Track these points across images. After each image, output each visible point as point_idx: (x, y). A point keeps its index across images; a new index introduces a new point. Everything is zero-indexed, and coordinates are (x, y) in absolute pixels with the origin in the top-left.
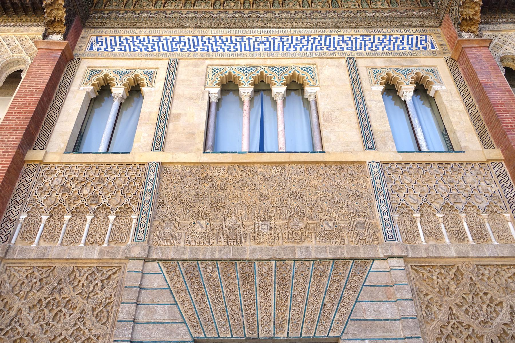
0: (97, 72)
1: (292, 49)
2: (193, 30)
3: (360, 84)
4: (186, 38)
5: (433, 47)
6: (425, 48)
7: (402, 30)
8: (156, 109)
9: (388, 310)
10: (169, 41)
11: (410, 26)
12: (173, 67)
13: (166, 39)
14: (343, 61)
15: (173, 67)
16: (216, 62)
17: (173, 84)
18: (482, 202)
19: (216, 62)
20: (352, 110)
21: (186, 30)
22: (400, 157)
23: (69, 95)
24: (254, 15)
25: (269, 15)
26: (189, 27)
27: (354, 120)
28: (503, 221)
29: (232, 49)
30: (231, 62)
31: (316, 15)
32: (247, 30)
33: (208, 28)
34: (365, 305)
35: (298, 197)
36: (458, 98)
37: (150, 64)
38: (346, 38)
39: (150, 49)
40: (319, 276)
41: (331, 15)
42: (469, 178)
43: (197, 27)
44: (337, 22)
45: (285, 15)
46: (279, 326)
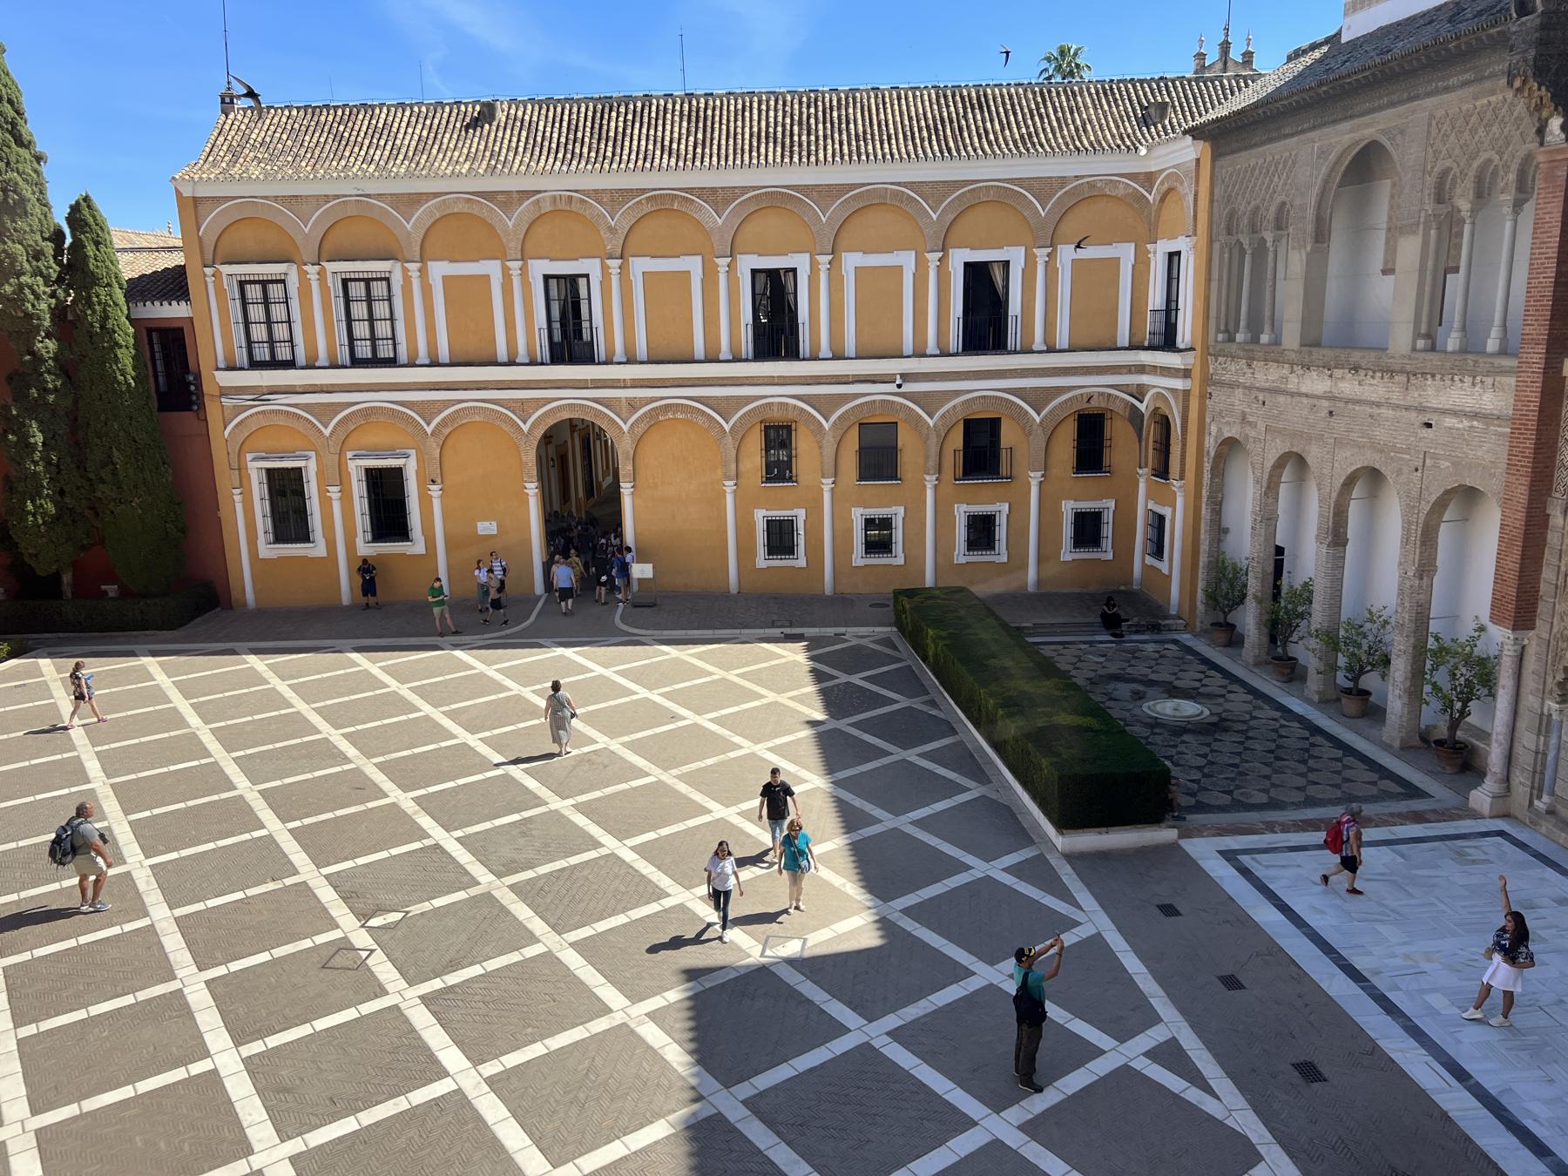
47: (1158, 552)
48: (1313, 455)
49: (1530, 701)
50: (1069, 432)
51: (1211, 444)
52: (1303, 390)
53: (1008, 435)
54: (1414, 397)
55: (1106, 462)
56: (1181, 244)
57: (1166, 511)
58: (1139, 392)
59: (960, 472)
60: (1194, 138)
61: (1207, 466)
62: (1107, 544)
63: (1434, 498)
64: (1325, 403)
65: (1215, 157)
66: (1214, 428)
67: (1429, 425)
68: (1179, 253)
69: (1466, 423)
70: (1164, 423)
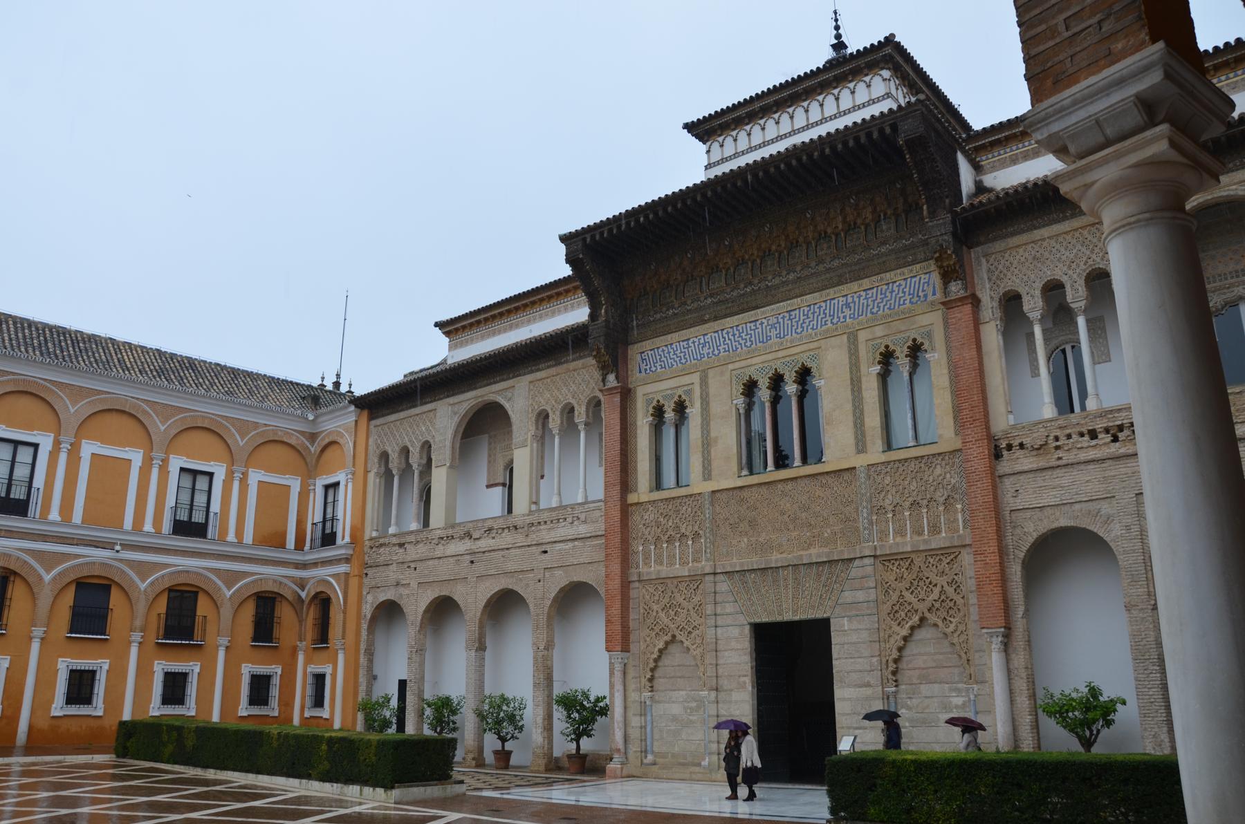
1: (799, 330)
2: (711, 324)
3: (859, 370)
5: (934, 294)
6: (925, 296)
7: (905, 270)
9: (860, 595)
11: (914, 262)
12: (704, 382)
14: (845, 337)
15: (704, 382)
16: (737, 365)
17: (708, 403)
18: (940, 496)
19: (737, 365)
20: (849, 407)
22: (883, 458)
23: (639, 432)
24: (762, 285)
25: (777, 281)
27: (851, 418)
28: (956, 511)
30: (749, 362)
31: (821, 268)
33: (726, 316)
34: (846, 594)
36: (946, 371)
37: (686, 380)
38: (850, 300)
40: (819, 576)
41: (836, 263)
42: (938, 471)
43: (716, 318)
44: (840, 276)
45: (791, 276)
46: (795, 612)
47: (319, 702)
48: (458, 593)
49: (633, 696)
50: (249, 611)
51: (368, 610)
52: (448, 552)
53: (203, 607)
54: (533, 538)
55: (276, 633)
56: (340, 477)
57: (328, 670)
58: (302, 584)
59: (162, 632)
60: (356, 406)
61: (365, 626)
62: (274, 702)
63: (553, 595)
64: (468, 558)
65: (371, 418)
66: (370, 598)
67: (545, 552)
68: (337, 484)
69: (570, 545)
70: (323, 602)
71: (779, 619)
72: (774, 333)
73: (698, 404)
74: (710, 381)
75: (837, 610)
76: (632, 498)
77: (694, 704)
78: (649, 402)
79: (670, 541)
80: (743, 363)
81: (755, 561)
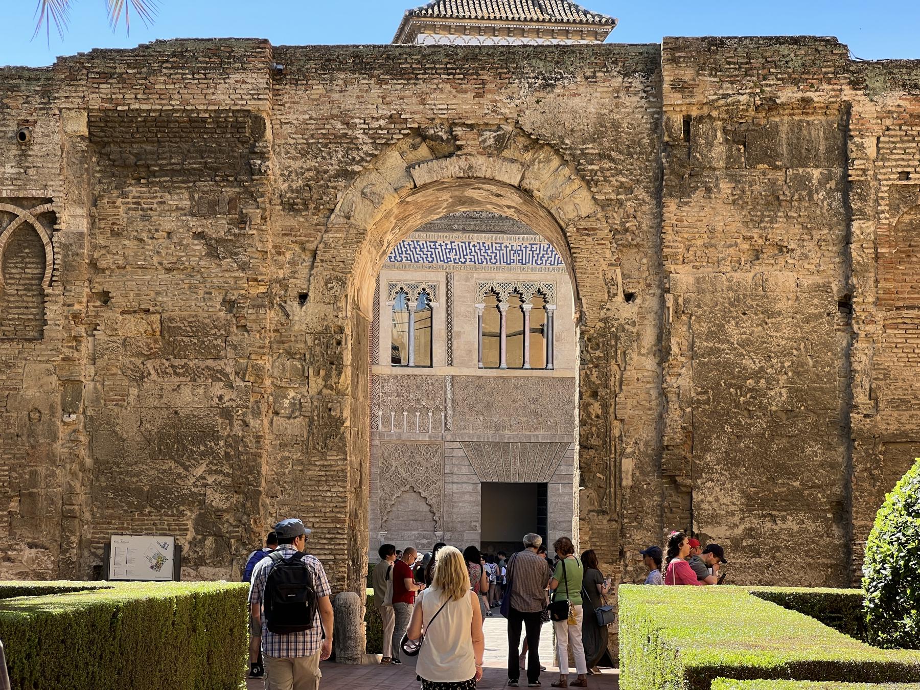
0: (395, 286)
1: (539, 262)
2: (460, 234)
4: (456, 244)
8: (443, 327)
10: (443, 248)
13: (441, 245)
16: (482, 276)
21: (456, 234)
26: (457, 230)
29: (493, 261)
32: (505, 236)
35: (534, 401)
39: (430, 260)
43: (464, 230)
46: (521, 477)
71: (508, 481)
72: (516, 258)
73: (443, 300)
74: (455, 283)
75: (554, 478)
76: (376, 370)
77: (425, 541)
78: (392, 286)
79: (412, 410)
80: (487, 276)
81: (489, 435)
